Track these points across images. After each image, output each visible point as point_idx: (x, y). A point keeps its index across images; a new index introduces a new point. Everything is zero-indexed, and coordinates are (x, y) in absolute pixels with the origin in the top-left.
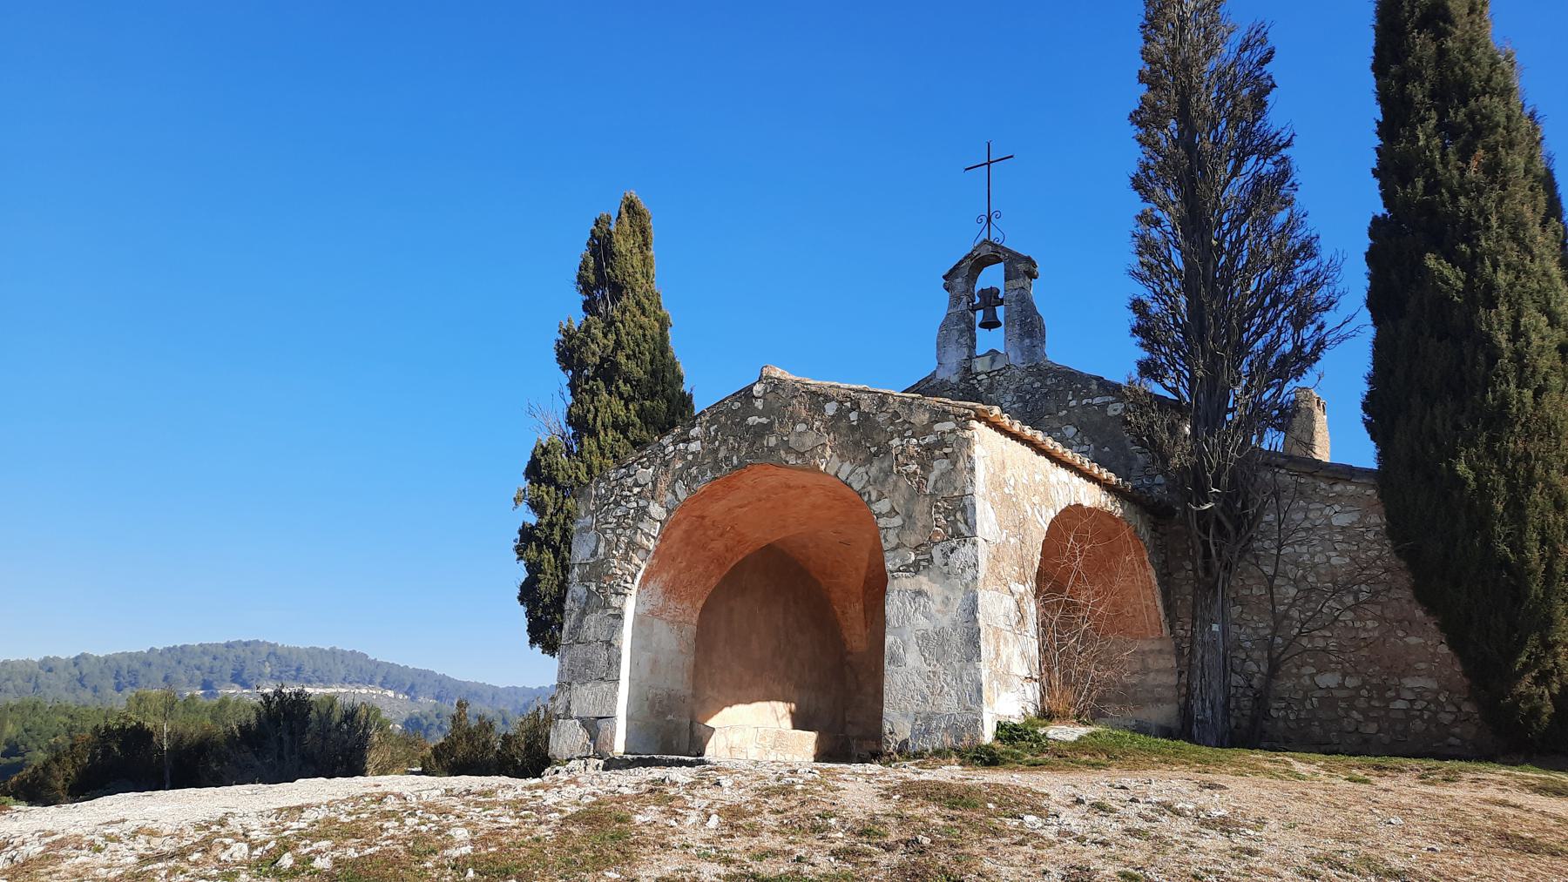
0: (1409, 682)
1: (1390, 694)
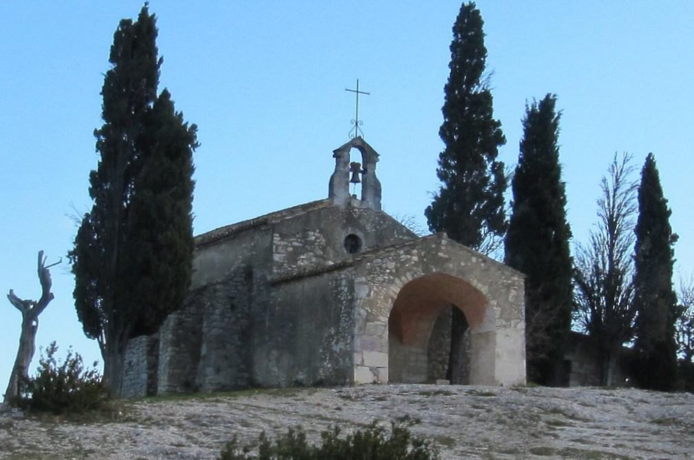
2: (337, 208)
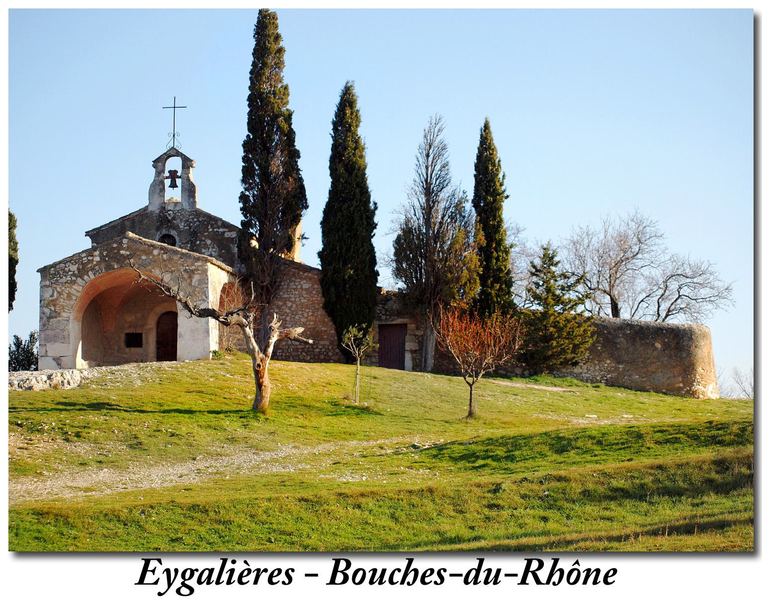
0: (322, 343)
1: (315, 347)
2: (152, 212)
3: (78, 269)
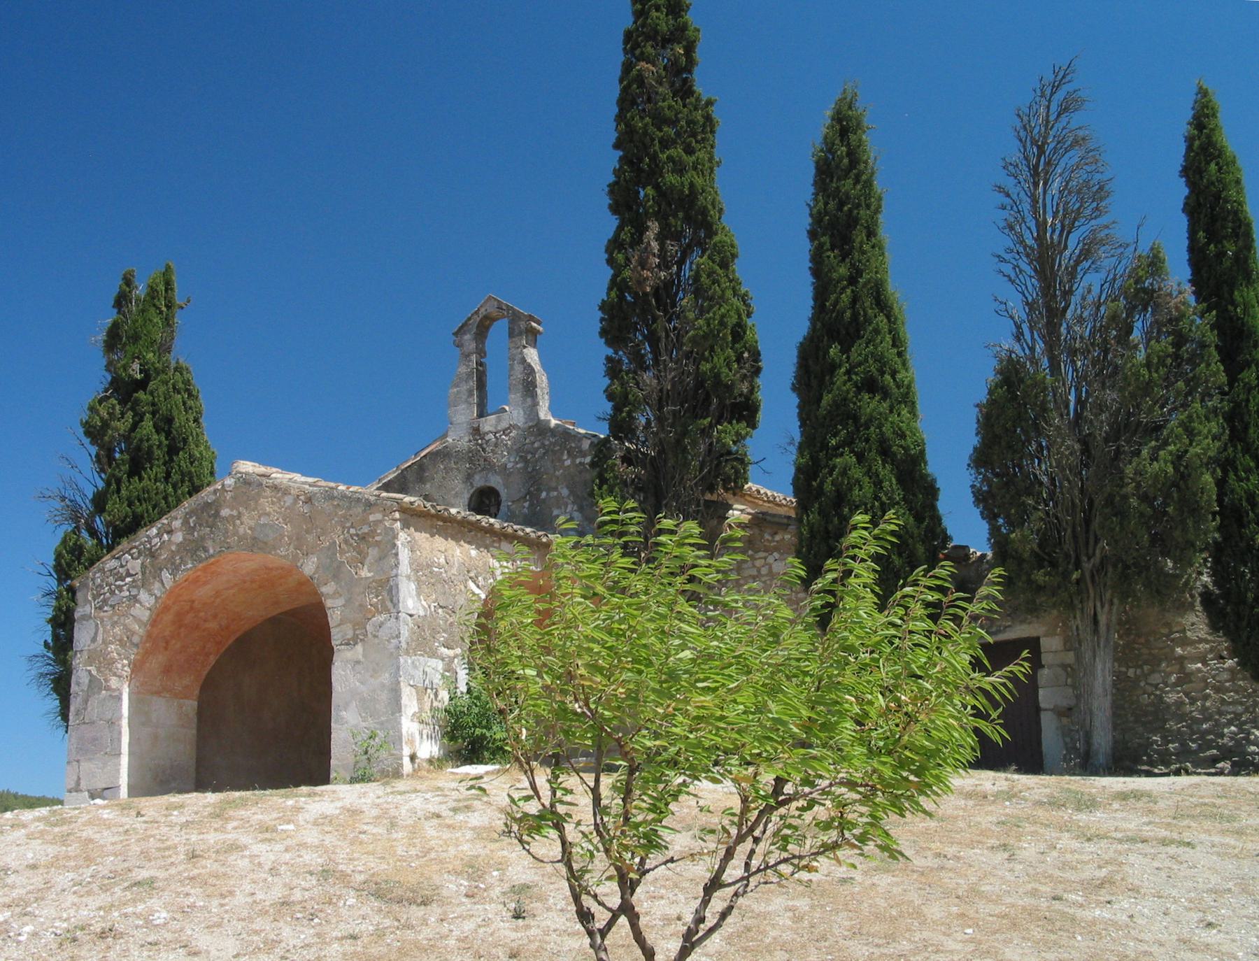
3: (143, 565)
